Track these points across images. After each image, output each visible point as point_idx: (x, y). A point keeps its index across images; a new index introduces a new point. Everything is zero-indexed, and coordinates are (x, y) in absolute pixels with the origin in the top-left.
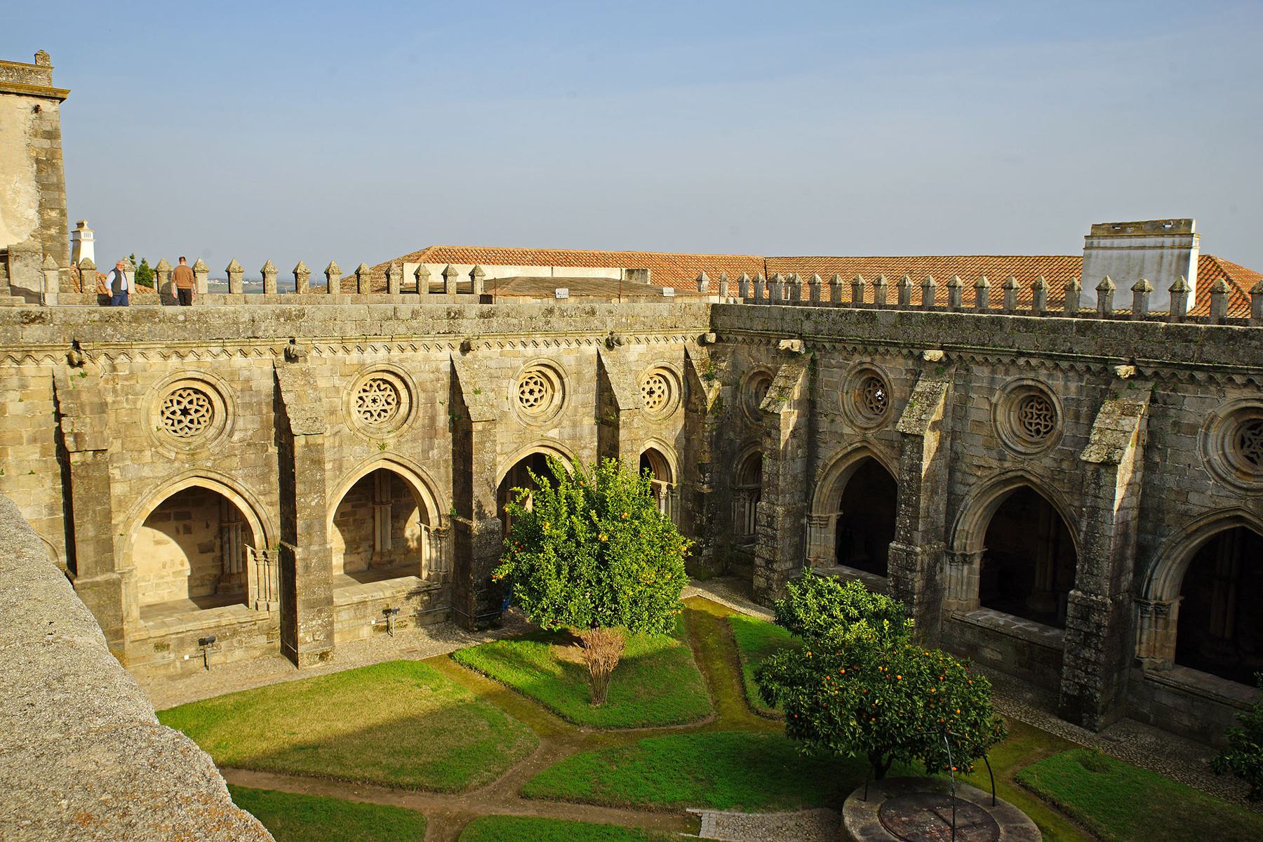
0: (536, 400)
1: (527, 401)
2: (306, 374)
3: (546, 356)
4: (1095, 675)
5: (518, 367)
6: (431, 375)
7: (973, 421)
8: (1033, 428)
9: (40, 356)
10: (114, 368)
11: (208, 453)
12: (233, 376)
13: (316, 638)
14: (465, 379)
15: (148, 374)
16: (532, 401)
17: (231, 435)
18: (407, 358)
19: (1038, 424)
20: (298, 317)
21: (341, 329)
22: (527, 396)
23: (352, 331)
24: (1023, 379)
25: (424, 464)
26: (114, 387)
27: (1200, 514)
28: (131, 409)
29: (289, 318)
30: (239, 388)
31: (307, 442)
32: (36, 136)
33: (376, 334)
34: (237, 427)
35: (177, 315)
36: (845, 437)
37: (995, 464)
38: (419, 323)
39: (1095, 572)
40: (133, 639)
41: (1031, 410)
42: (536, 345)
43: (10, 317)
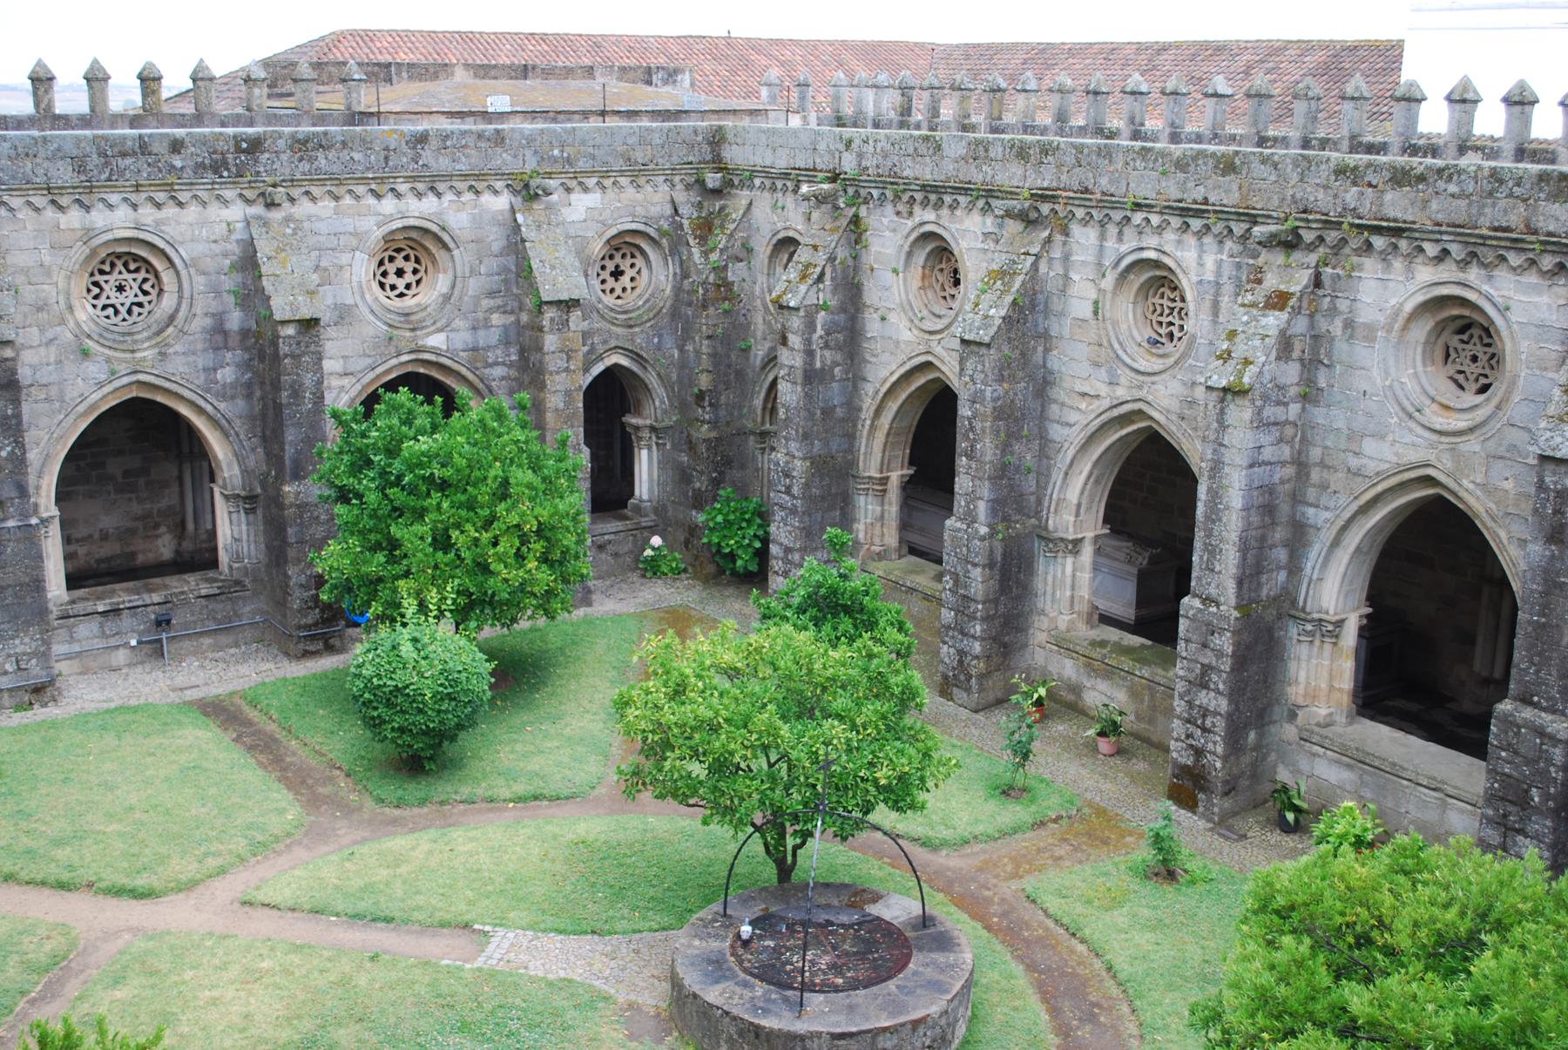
0: (408, 286)
1: (393, 287)
3: (417, 214)
4: (1215, 733)
7: (1074, 318)
8: (1163, 331)
16: (401, 289)
18: (168, 218)
19: (1171, 324)
22: (392, 279)
24: (1142, 249)
25: (208, 391)
27: (1378, 474)
36: (903, 346)
37: (1103, 390)
39: (1218, 568)
41: (1161, 301)
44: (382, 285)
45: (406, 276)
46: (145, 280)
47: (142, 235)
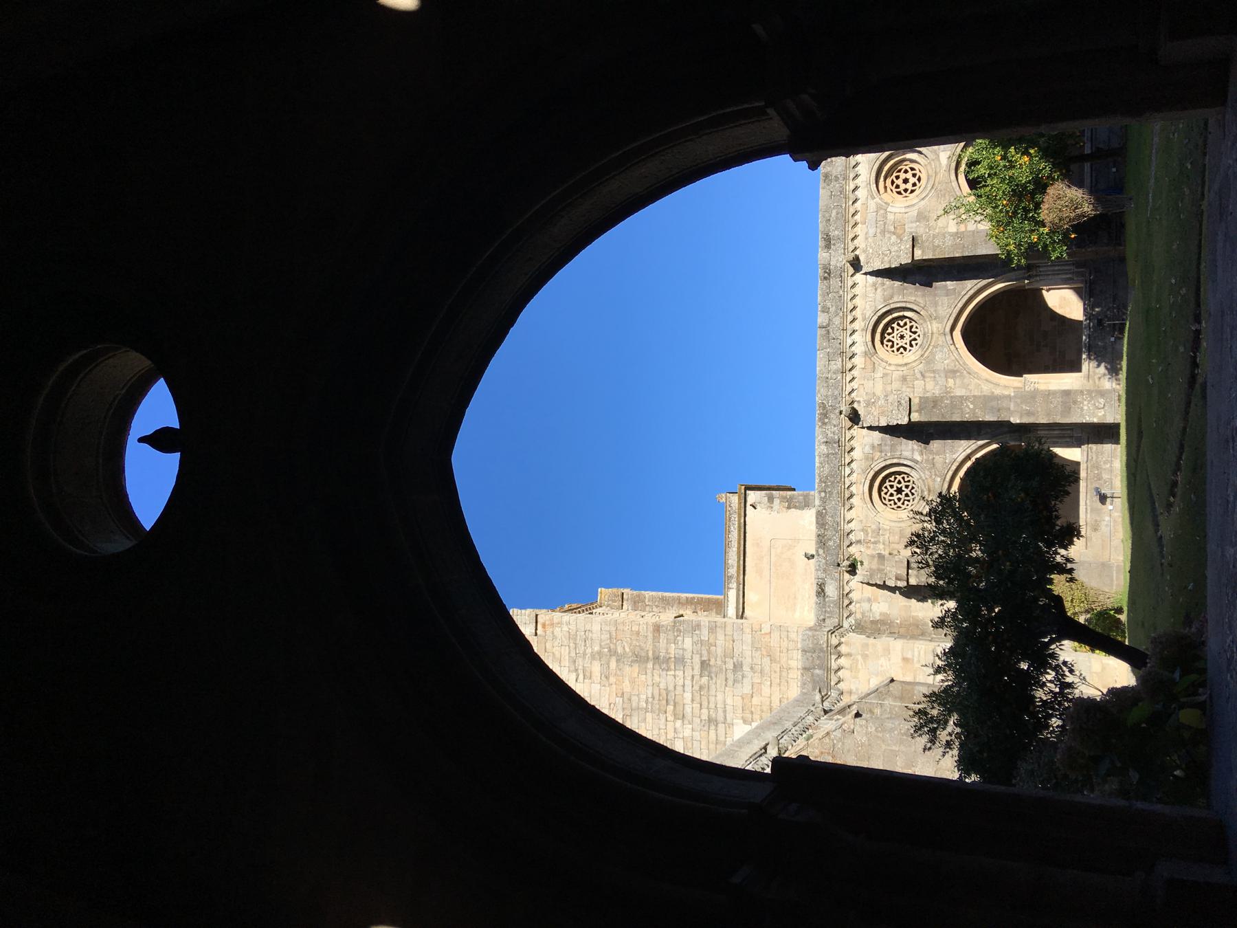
2: (868, 404)
3: (869, 176)
5: (877, 204)
6: (879, 290)
9: (847, 590)
10: (859, 542)
11: (929, 480)
12: (869, 458)
13: (1102, 406)
14: (879, 263)
15: (864, 521)
17: (916, 462)
18: (862, 314)
20: (824, 407)
21: (834, 373)
22: (909, 186)
23: (837, 365)
25: (960, 293)
26: (873, 543)
28: (890, 533)
29: (825, 415)
30: (879, 454)
31: (916, 411)
32: (772, 507)
33: (840, 343)
34: (910, 457)
35: (821, 498)
38: (832, 305)
40: (1084, 548)
42: (856, 188)
43: (820, 603)
44: (912, 191)
45: (904, 178)
46: (898, 324)
47: (870, 328)
